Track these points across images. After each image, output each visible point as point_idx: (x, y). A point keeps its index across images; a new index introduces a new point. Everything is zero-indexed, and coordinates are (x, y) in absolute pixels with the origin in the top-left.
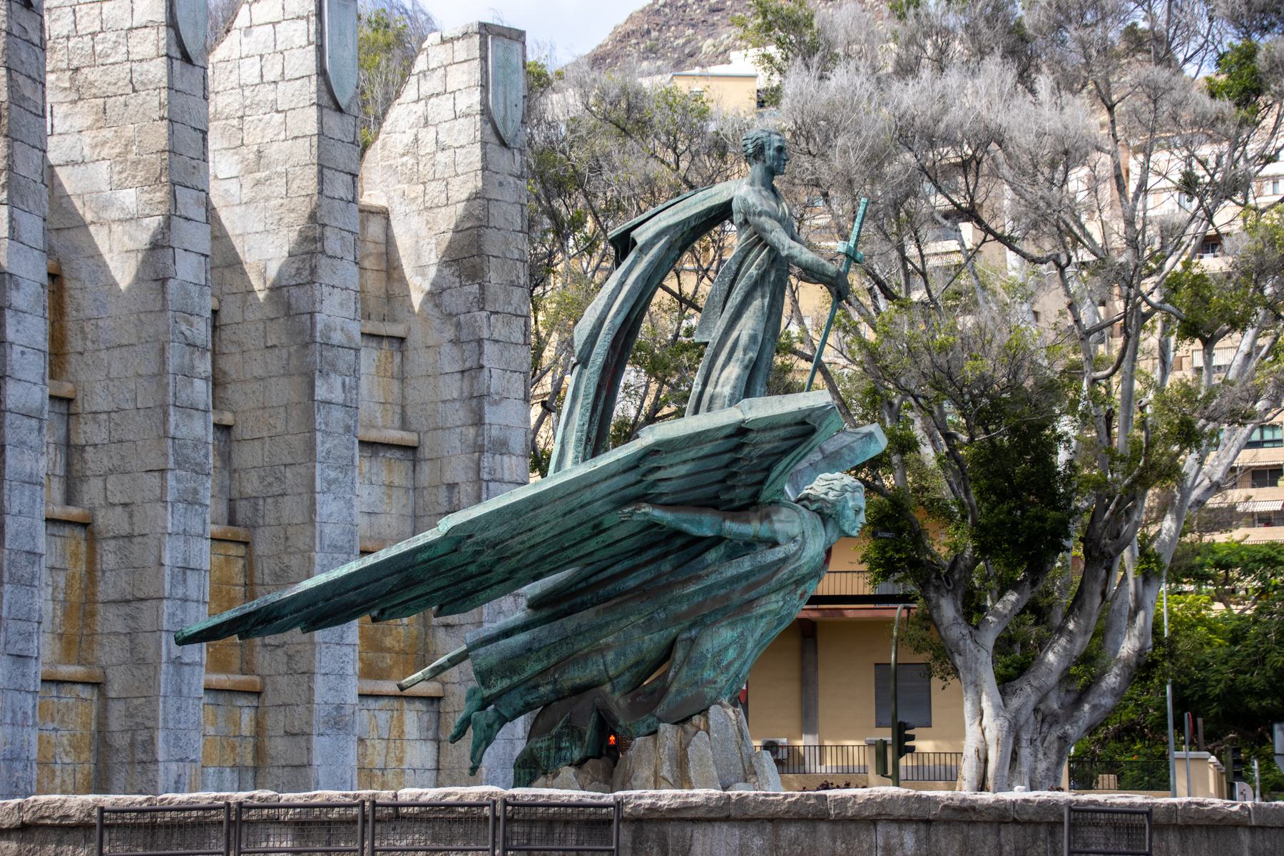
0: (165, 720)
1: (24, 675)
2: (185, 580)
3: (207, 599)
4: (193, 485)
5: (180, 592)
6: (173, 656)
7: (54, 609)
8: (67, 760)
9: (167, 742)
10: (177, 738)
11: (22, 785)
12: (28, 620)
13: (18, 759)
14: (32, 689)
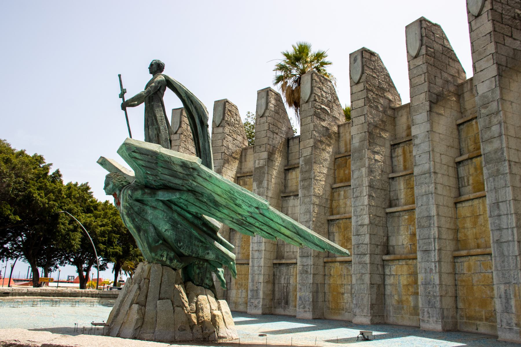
0: (496, 267)
1: (429, 257)
2: (498, 207)
4: (496, 168)
5: (496, 213)
9: (497, 275)
10: (503, 274)
11: (432, 293)
12: (429, 238)
13: (429, 284)
14: (433, 260)
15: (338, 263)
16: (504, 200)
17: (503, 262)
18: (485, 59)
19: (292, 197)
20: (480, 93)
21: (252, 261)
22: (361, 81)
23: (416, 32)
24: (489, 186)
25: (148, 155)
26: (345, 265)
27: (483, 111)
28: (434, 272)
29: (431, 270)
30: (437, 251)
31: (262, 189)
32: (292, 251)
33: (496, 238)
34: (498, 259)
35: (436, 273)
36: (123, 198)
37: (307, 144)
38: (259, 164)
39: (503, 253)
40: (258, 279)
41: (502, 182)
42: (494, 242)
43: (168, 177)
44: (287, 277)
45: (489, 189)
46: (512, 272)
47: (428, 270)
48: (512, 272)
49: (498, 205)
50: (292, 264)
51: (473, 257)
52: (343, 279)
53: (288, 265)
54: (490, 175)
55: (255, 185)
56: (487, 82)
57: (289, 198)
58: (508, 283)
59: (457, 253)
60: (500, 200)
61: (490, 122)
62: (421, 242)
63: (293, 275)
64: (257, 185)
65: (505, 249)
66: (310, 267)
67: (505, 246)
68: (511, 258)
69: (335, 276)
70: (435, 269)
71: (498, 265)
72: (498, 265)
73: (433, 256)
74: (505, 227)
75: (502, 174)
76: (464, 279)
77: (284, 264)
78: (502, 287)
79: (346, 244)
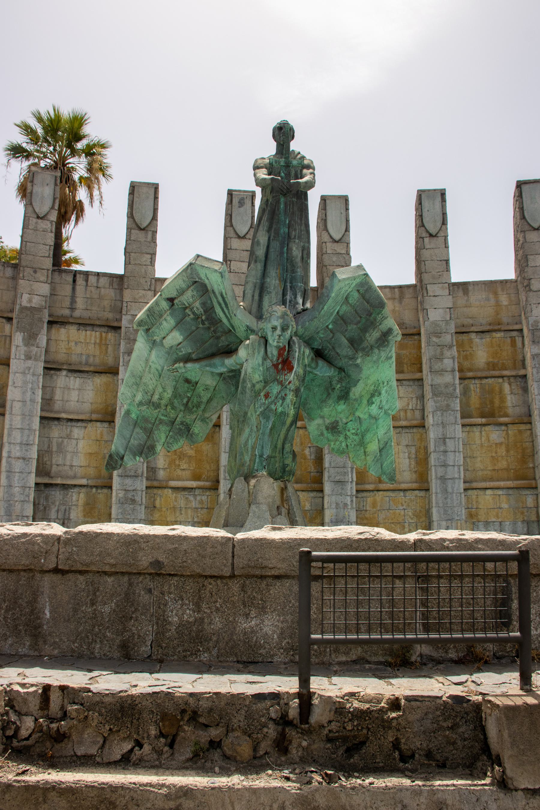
0: (437, 503)
1: (343, 489)
2: (445, 443)
3: (461, 450)
5: (442, 448)
6: (439, 476)
7: (410, 462)
8: (411, 521)
9: (438, 512)
10: (445, 511)
12: (344, 467)
14: (349, 494)
15: (170, 490)
16: (453, 436)
17: (446, 499)
18: (440, 285)
19: (64, 373)
20: (431, 319)
21: (8, 477)
22: (248, 236)
23: (342, 211)
24: (435, 419)
25: (368, 303)
26: (183, 493)
27: (434, 339)
28: (349, 507)
29: (346, 505)
30: (354, 483)
31: (34, 349)
32: (68, 463)
33: (439, 475)
34: (440, 495)
35: (352, 508)
36: (298, 360)
37: (141, 297)
38: (30, 301)
39: (446, 490)
40: (22, 510)
41: (452, 419)
42: (436, 478)
43: (346, 341)
44: (63, 508)
45: (436, 423)
46: (456, 509)
47: (341, 505)
48: (456, 509)
49: (444, 440)
50: (75, 486)
51: (381, 493)
52: (178, 514)
53: (65, 487)
54: (438, 409)
55: (20, 338)
56: (441, 310)
57: (58, 373)
58: (450, 520)
59: (361, 487)
60: (448, 436)
61: (442, 354)
62: (332, 471)
63: (76, 505)
64: (24, 339)
65: (450, 486)
66: (140, 493)
67: (449, 484)
68: (454, 495)
69: (164, 509)
70: (352, 504)
71: (440, 502)
72: (440, 502)
73: (349, 488)
74: (451, 464)
75: (452, 411)
76: (367, 515)
77: (56, 485)
78: (444, 523)
79: (177, 462)
